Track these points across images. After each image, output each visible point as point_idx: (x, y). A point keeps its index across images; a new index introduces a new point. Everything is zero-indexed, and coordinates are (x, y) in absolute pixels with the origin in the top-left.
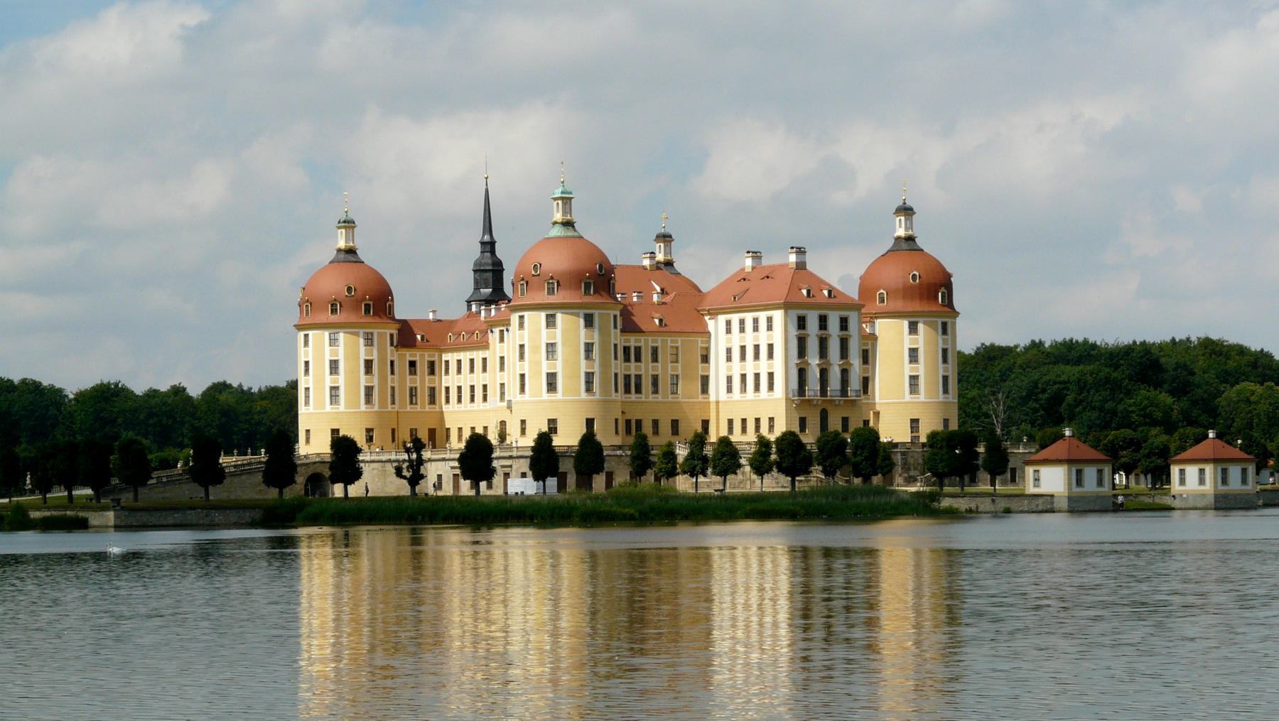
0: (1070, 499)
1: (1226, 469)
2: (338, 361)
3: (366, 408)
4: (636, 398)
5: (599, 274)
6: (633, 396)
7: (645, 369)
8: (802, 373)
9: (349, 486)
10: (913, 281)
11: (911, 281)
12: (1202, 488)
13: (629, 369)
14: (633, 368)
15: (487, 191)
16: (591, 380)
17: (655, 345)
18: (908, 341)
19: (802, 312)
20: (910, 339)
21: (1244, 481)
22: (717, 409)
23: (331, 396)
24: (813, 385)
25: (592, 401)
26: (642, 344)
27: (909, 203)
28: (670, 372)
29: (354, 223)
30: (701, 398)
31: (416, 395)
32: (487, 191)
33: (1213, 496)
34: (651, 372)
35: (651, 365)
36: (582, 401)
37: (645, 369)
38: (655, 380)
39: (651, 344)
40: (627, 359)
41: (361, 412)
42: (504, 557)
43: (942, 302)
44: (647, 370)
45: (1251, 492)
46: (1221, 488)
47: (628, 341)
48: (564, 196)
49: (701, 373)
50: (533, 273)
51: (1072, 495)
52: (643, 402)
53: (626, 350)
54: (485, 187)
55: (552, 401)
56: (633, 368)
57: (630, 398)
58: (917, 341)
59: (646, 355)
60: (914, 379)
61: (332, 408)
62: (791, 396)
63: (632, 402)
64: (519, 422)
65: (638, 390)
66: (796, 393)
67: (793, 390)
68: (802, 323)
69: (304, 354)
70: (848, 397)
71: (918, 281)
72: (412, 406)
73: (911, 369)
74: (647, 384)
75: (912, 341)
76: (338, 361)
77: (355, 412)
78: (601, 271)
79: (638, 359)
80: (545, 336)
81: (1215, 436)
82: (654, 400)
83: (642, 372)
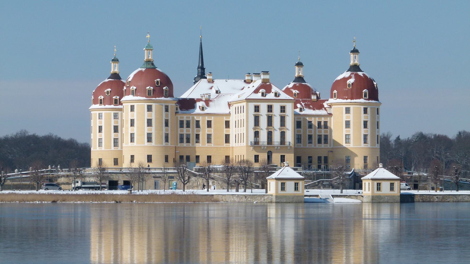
0: (276, 197)
1: (284, 183)
2: (118, 126)
3: (114, 149)
4: (186, 145)
5: (156, 86)
6: (185, 144)
7: (192, 131)
8: (257, 134)
9: (80, 186)
10: (349, 87)
11: (348, 87)
12: (392, 192)
13: (183, 131)
14: (185, 131)
15: (201, 43)
16: (182, 137)
17: (188, 119)
18: (345, 117)
19: (257, 104)
20: (364, 116)
21: (392, 189)
22: (233, 150)
23: (114, 142)
24: (263, 138)
25: (150, 147)
26: (191, 119)
27: (356, 48)
28: (179, 132)
29: (118, 60)
30: (225, 145)
31: (101, 143)
32: (201, 43)
33: (371, 197)
34: (195, 133)
35: (179, 129)
36: (144, 147)
37: (192, 131)
38: (198, 136)
39: (179, 119)
40: (182, 126)
41: (111, 151)
42: (228, 222)
43: (365, 97)
44: (193, 131)
45: (396, 195)
46: (377, 193)
47: (183, 118)
48: (148, 48)
49: (225, 133)
50: (156, 85)
51: (278, 195)
52: (190, 147)
53: (182, 122)
54: (200, 41)
55: (132, 147)
56: (185, 131)
57: (183, 145)
58: (349, 117)
59: (193, 125)
60: (365, 136)
61: (99, 149)
62: (249, 144)
63: (184, 147)
64: (130, 157)
65: (188, 141)
66: (253, 143)
67: (251, 142)
68: (257, 109)
69: (95, 123)
70: (285, 145)
71: (351, 87)
72: (99, 148)
73: (346, 131)
74: (193, 138)
75: (347, 117)
76: (118, 126)
77: (109, 151)
78: (158, 85)
79: (188, 126)
80: (147, 116)
81: (382, 167)
82: (208, 146)
83: (191, 133)
